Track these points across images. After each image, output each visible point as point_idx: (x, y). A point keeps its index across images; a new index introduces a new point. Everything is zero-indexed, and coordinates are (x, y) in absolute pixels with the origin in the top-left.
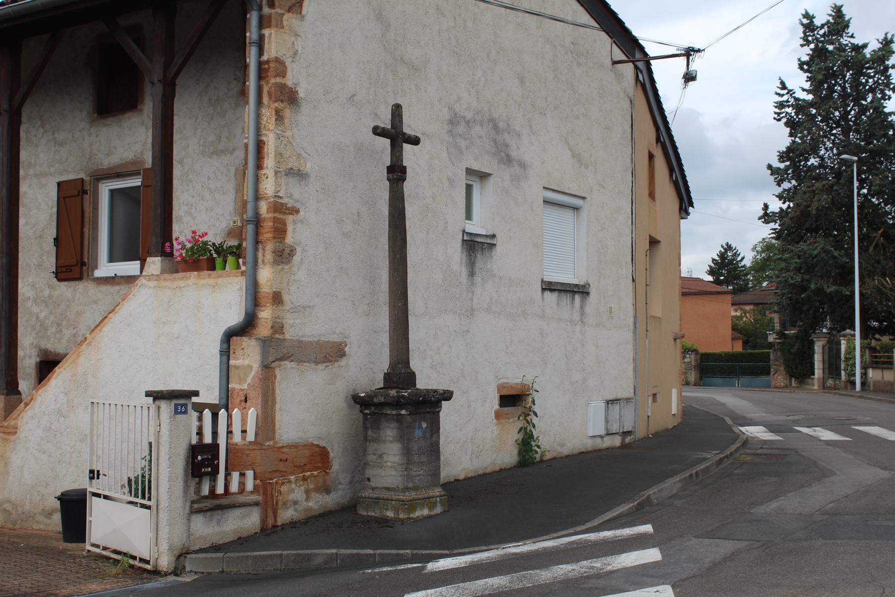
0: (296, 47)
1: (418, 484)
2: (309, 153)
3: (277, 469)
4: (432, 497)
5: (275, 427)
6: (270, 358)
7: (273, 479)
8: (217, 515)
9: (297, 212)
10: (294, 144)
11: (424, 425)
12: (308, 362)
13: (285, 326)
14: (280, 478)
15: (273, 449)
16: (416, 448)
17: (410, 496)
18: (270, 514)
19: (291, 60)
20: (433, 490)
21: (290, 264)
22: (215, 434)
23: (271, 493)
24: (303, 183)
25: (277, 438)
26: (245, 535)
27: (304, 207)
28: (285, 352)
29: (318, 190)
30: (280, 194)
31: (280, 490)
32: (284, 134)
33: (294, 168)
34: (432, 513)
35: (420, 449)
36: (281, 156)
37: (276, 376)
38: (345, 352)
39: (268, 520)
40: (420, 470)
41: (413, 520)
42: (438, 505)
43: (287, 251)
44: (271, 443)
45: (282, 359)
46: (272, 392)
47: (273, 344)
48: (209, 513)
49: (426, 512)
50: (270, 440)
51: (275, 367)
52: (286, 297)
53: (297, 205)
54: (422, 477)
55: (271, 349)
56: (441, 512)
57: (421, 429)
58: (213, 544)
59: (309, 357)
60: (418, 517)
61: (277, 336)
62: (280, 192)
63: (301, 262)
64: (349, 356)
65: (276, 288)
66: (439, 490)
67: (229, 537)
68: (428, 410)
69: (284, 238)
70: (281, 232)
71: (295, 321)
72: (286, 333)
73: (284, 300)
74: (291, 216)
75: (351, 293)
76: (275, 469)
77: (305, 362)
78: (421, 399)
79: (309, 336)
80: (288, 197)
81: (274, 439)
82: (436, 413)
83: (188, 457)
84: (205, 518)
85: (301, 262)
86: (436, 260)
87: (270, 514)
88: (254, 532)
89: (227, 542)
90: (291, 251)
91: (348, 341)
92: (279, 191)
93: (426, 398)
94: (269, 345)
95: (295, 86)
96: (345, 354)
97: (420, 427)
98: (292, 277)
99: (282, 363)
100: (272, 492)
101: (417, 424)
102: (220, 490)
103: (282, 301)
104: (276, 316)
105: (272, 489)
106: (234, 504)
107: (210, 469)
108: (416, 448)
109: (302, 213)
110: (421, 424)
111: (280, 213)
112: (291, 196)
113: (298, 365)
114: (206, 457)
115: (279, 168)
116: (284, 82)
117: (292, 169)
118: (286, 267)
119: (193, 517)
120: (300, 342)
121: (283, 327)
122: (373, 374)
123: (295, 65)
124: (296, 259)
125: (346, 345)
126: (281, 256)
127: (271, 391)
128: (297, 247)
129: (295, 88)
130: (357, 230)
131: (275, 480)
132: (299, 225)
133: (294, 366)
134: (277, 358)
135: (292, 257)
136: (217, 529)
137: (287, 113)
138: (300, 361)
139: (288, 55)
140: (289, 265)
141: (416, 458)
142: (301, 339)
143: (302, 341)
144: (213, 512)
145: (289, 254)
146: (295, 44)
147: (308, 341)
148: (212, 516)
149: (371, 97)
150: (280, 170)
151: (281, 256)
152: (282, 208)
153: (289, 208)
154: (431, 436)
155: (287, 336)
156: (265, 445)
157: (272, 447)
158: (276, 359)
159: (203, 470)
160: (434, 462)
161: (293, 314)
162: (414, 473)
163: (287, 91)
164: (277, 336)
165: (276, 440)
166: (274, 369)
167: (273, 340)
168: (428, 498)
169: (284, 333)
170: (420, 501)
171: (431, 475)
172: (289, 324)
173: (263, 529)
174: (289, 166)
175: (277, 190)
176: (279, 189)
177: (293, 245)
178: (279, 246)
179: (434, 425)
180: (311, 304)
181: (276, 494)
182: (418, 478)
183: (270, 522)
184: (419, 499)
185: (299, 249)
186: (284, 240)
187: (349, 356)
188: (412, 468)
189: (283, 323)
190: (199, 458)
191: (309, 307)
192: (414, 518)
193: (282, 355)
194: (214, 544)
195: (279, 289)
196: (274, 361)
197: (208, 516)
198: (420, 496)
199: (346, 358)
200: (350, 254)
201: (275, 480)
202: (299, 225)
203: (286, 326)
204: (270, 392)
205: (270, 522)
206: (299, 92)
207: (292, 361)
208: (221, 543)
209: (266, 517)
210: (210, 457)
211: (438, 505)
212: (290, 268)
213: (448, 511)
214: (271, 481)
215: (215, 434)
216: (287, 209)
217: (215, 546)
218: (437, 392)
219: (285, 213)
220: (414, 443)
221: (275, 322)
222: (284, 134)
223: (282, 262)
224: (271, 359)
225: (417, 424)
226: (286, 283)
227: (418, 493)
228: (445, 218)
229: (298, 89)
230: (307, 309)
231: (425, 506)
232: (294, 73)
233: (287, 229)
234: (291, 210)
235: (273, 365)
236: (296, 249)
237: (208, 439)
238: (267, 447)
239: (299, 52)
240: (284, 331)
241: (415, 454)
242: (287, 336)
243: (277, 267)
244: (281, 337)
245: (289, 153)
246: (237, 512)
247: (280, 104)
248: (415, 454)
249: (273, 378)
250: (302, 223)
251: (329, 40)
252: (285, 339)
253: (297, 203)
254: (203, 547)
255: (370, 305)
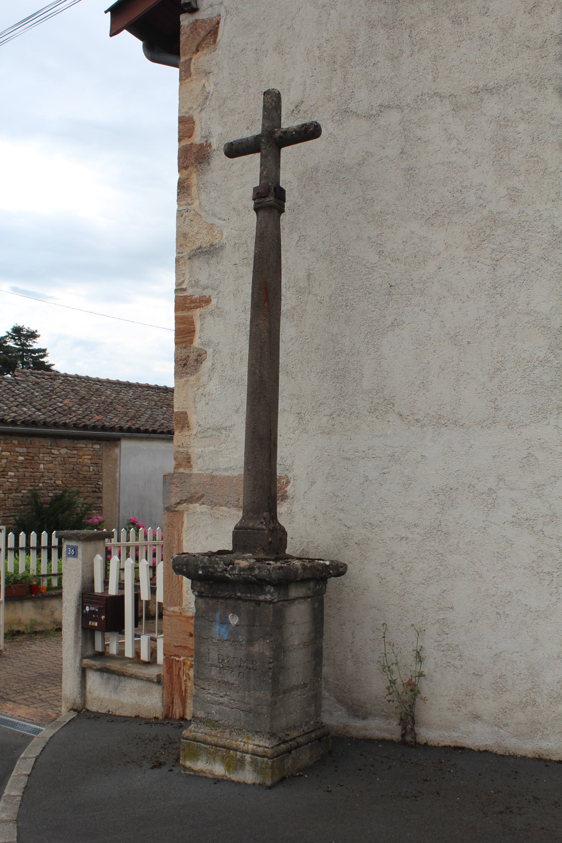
0: (207, 90)
1: (217, 717)
2: (223, 218)
3: (185, 645)
4: (236, 750)
5: (182, 590)
6: (173, 499)
7: (179, 657)
8: (114, 680)
9: (208, 301)
10: (203, 214)
11: (234, 620)
12: (226, 505)
13: (192, 456)
14: (190, 658)
15: (180, 618)
16: (214, 655)
17: (194, 732)
18: (177, 701)
19: (200, 109)
20: (248, 738)
21: (198, 373)
22: (121, 586)
23: (177, 673)
24: (213, 261)
25: (184, 604)
26: (144, 714)
27: (216, 293)
28: (193, 491)
29: (238, 262)
30: (184, 286)
31: (188, 674)
32: (189, 208)
33: (204, 245)
34: (235, 777)
35: (223, 660)
36: (184, 237)
37: (183, 522)
38: (286, 492)
39: (175, 707)
40: (222, 694)
41: (192, 773)
42: (248, 767)
43: (193, 356)
44: (176, 609)
45: (190, 500)
46: (178, 543)
47: (175, 480)
48: (105, 675)
49: (219, 769)
50: (175, 605)
51: (183, 511)
52: (193, 419)
53: (207, 293)
54: (227, 709)
55: (173, 487)
56: (254, 784)
57: (225, 626)
58: (109, 711)
59: (226, 498)
60: (202, 771)
61: (181, 470)
62: (184, 284)
63: (213, 368)
64: (292, 498)
65: (178, 408)
66: (262, 743)
67: (126, 711)
68: (239, 594)
69: (191, 341)
70: (185, 334)
71: (206, 448)
72: (193, 466)
73: (190, 422)
74: (199, 309)
75: (295, 401)
76: (183, 645)
77: (221, 506)
78: (200, 572)
79: (226, 470)
80: (192, 286)
81: (180, 604)
82: (262, 604)
83: (79, 605)
84: (102, 678)
85: (213, 368)
86: (528, 314)
87: (177, 701)
88: (154, 716)
89: (123, 715)
90: (199, 355)
91: (290, 475)
92: (183, 282)
93: (212, 573)
94: (170, 482)
95: (205, 139)
96: (287, 496)
97: (225, 622)
98: (201, 391)
99: (191, 506)
100: (179, 673)
101: (218, 615)
102: (129, 653)
103: (188, 424)
104: (180, 444)
105: (180, 669)
106: (123, 672)
107: (96, 624)
108: (214, 655)
109: (214, 302)
110: (227, 617)
111: (183, 310)
112: (196, 284)
113: (211, 509)
114: (93, 609)
115: (182, 253)
116: (190, 143)
117: (200, 247)
118: (192, 378)
119: (90, 673)
120: (213, 477)
121: (190, 458)
122: (345, 528)
123: (203, 114)
124: (207, 365)
125: (288, 482)
126: (185, 365)
127: (176, 542)
128: (207, 349)
129: (206, 141)
130: (306, 303)
131: (182, 658)
132: (209, 319)
133: (204, 510)
134: (183, 499)
135: (201, 363)
136: (114, 697)
137: (194, 179)
138: (214, 504)
139: (195, 107)
140: (195, 376)
141: (214, 672)
142: (213, 474)
143: (217, 476)
144: (110, 676)
145: (196, 360)
146: (206, 86)
147: (225, 476)
148: (109, 679)
149: (334, 90)
150: (183, 255)
151: (185, 365)
152: (186, 303)
153: (196, 299)
154: (251, 642)
155: (195, 471)
156: (167, 610)
157: (177, 614)
158: (181, 500)
159: (90, 623)
160: (255, 690)
161: (203, 439)
162: (209, 697)
163: (194, 151)
164: (181, 470)
165: (183, 606)
166: (181, 513)
167: (175, 475)
168: (229, 748)
169: (191, 466)
170: (208, 747)
171: (249, 711)
172: (197, 454)
173: (166, 717)
174: (198, 244)
175: (180, 281)
176: (182, 279)
177: (201, 347)
178: (181, 353)
179: (257, 624)
180: (228, 424)
181: (185, 678)
182: (217, 707)
183: (178, 711)
184: (204, 742)
185: (210, 351)
186: (192, 343)
187: (292, 498)
188: (207, 688)
189: (189, 453)
190: (87, 609)
191: (225, 429)
192: (194, 771)
193: (189, 495)
194: (110, 713)
195: (184, 408)
196: (179, 503)
197: (104, 677)
198: (209, 739)
199: (288, 500)
200: (294, 341)
201: (182, 658)
202: (209, 319)
203: (194, 458)
204: (175, 542)
205: (178, 711)
206: (212, 145)
207: (203, 503)
208: (117, 713)
209: (173, 703)
210: (97, 610)
211: (248, 767)
212: (198, 379)
213: (269, 788)
214: (177, 659)
215: (121, 586)
216: (192, 302)
217: (110, 714)
218: (233, 564)
219: (190, 308)
220: (211, 647)
221: (177, 452)
222: (189, 208)
223: (187, 373)
224: (174, 500)
225: (218, 615)
226: (193, 400)
227: (213, 732)
228: (553, 226)
229: (211, 140)
230: (223, 431)
231: (217, 758)
232: (203, 124)
233: (194, 328)
234: (199, 302)
235: (180, 508)
236: (206, 352)
237: (113, 591)
238: (172, 613)
239: (211, 93)
240: (192, 463)
241: (212, 665)
242: (195, 471)
243: (180, 380)
244: (187, 471)
245: (196, 229)
246: (136, 684)
247: (184, 171)
248: (212, 665)
249: (180, 525)
250: (212, 313)
251: (256, 50)
252: (191, 475)
253: (206, 290)
254: (100, 711)
255: (335, 416)
